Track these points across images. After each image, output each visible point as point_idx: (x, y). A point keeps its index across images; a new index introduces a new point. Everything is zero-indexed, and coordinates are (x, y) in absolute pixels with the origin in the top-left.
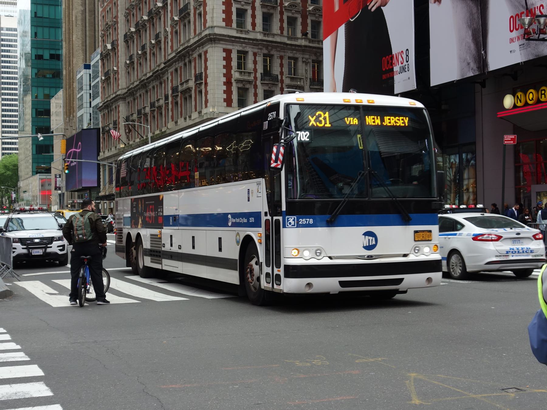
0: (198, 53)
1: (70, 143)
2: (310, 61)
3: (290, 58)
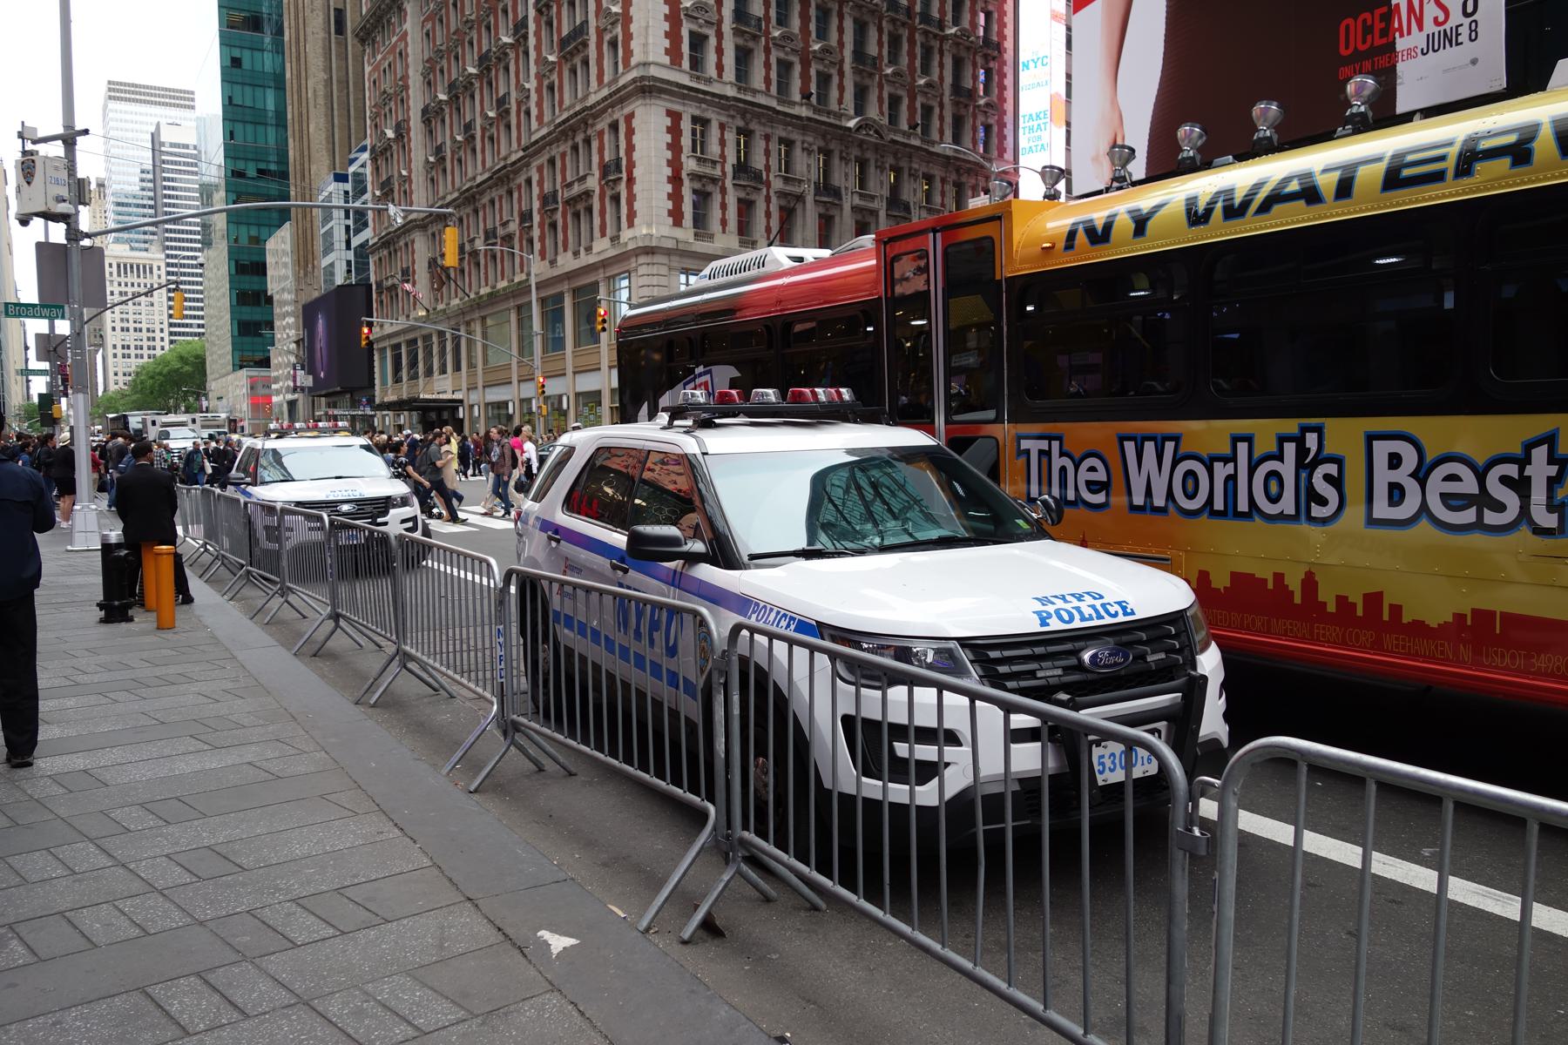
0: (609, 120)
1: (308, 314)
2: (815, 148)
3: (781, 141)
